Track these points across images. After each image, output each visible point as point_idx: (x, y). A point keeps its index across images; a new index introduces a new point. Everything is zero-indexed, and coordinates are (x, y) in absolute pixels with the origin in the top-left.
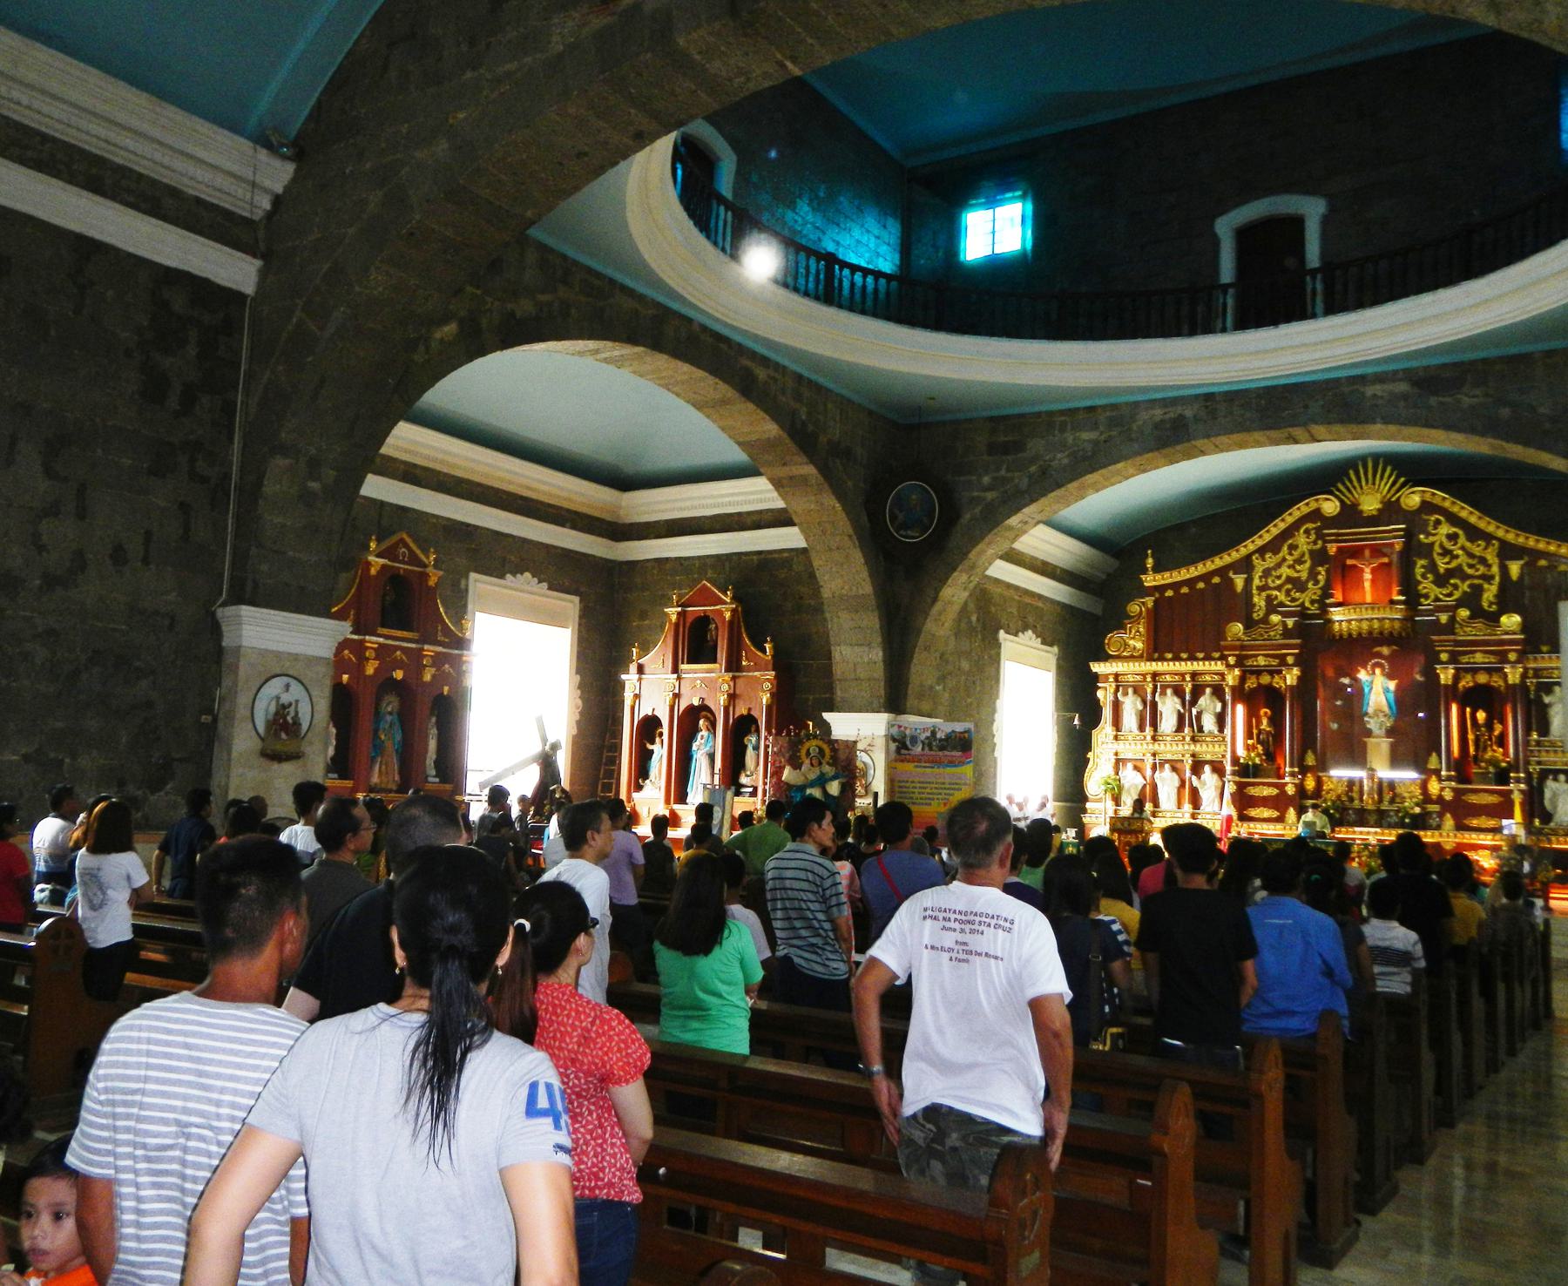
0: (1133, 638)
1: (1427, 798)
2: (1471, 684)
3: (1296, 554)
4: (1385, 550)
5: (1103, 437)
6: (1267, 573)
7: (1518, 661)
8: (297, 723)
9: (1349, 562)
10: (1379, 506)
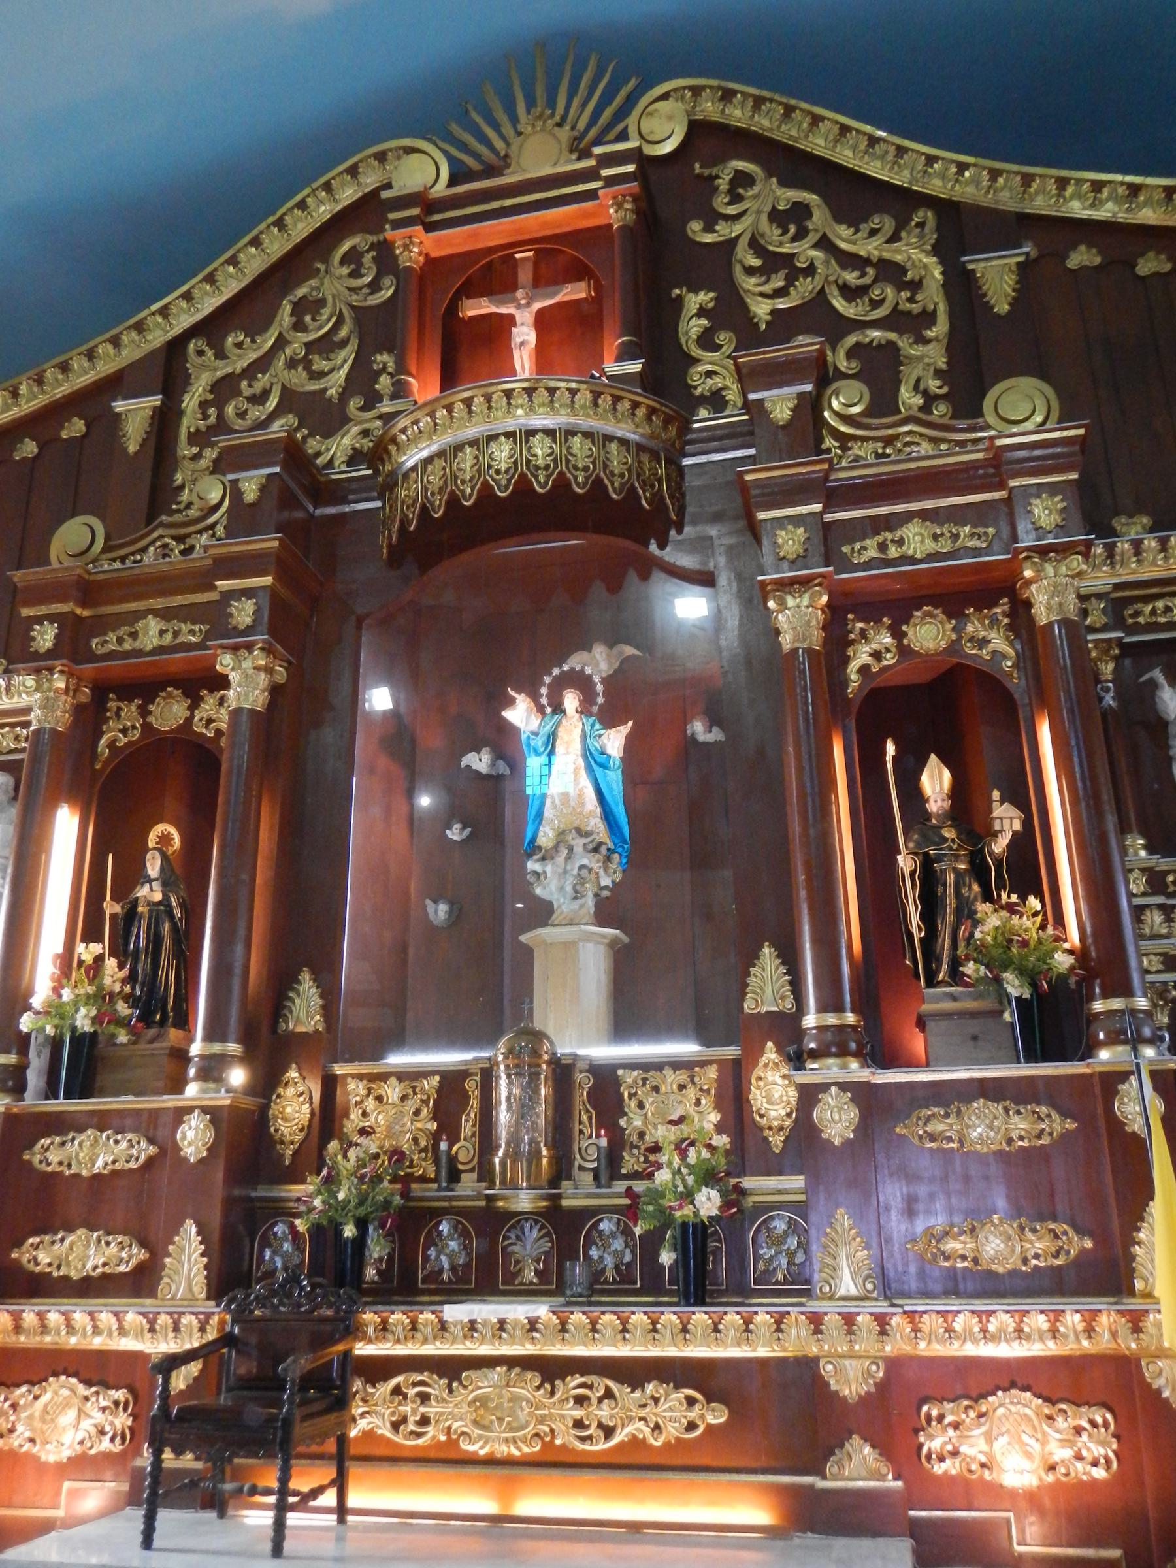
2: (889, 660)
6: (224, 389)
9: (476, 308)
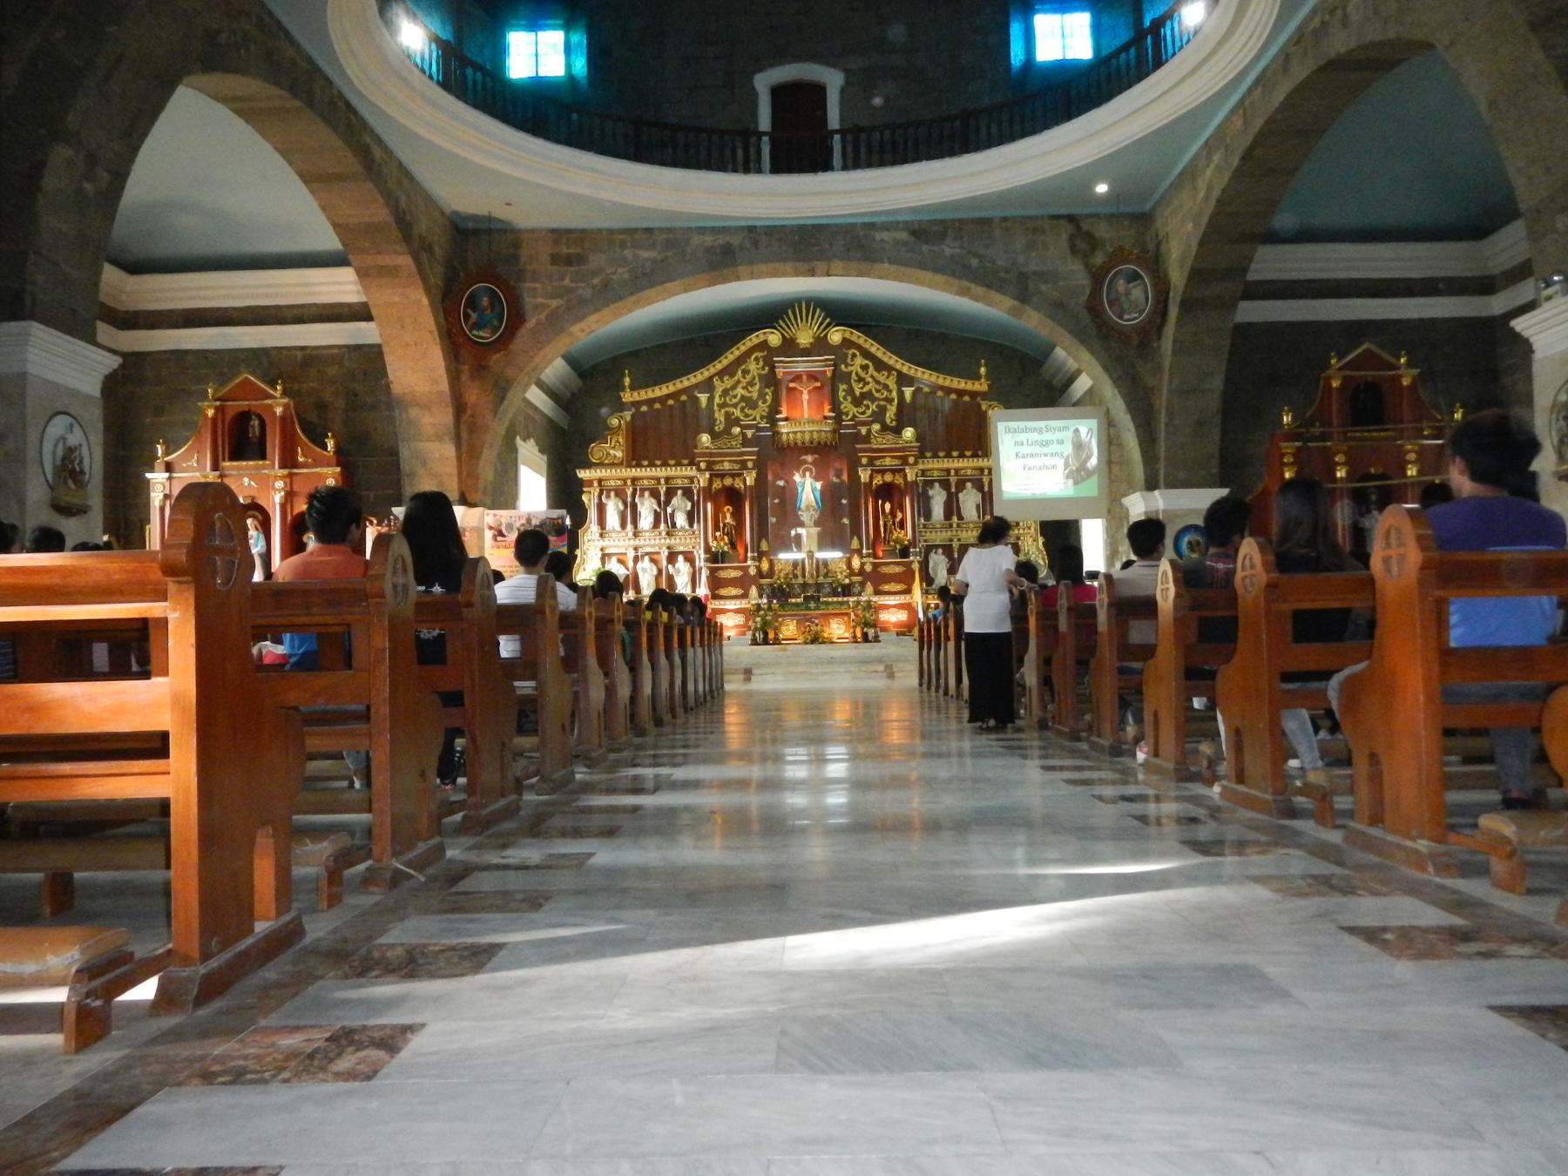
0: (614, 448)
1: (852, 573)
3: (748, 378)
4: (819, 376)
5: (659, 258)
6: (725, 392)
7: (916, 463)
8: (82, 472)
9: (791, 385)
10: (812, 340)
